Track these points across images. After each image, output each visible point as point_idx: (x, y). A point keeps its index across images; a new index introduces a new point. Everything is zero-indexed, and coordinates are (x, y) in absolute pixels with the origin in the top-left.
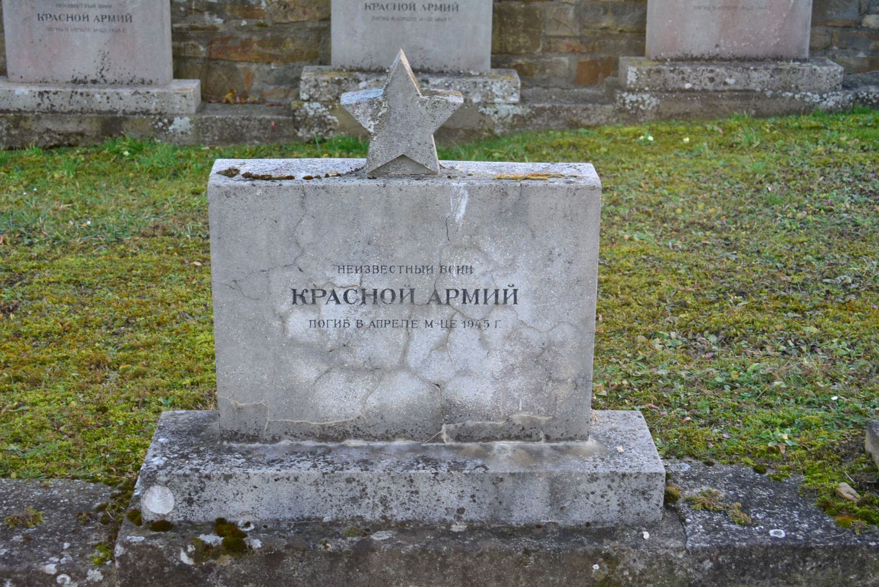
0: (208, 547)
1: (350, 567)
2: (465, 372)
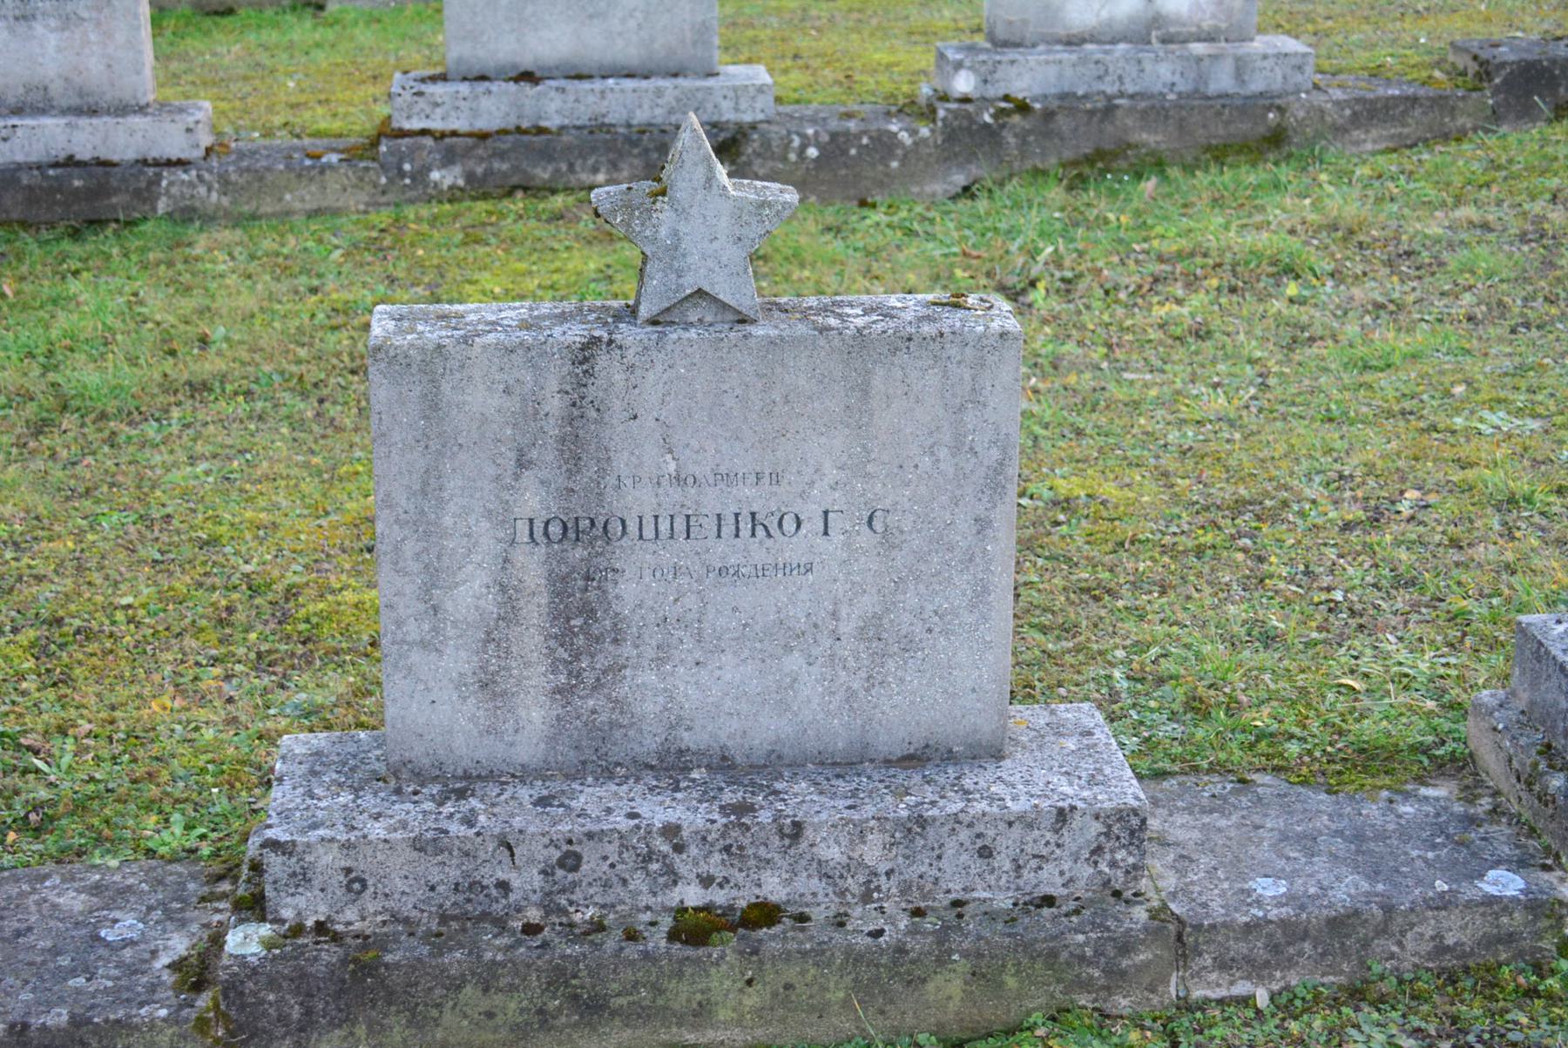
0: (1003, 110)
1: (1102, 121)
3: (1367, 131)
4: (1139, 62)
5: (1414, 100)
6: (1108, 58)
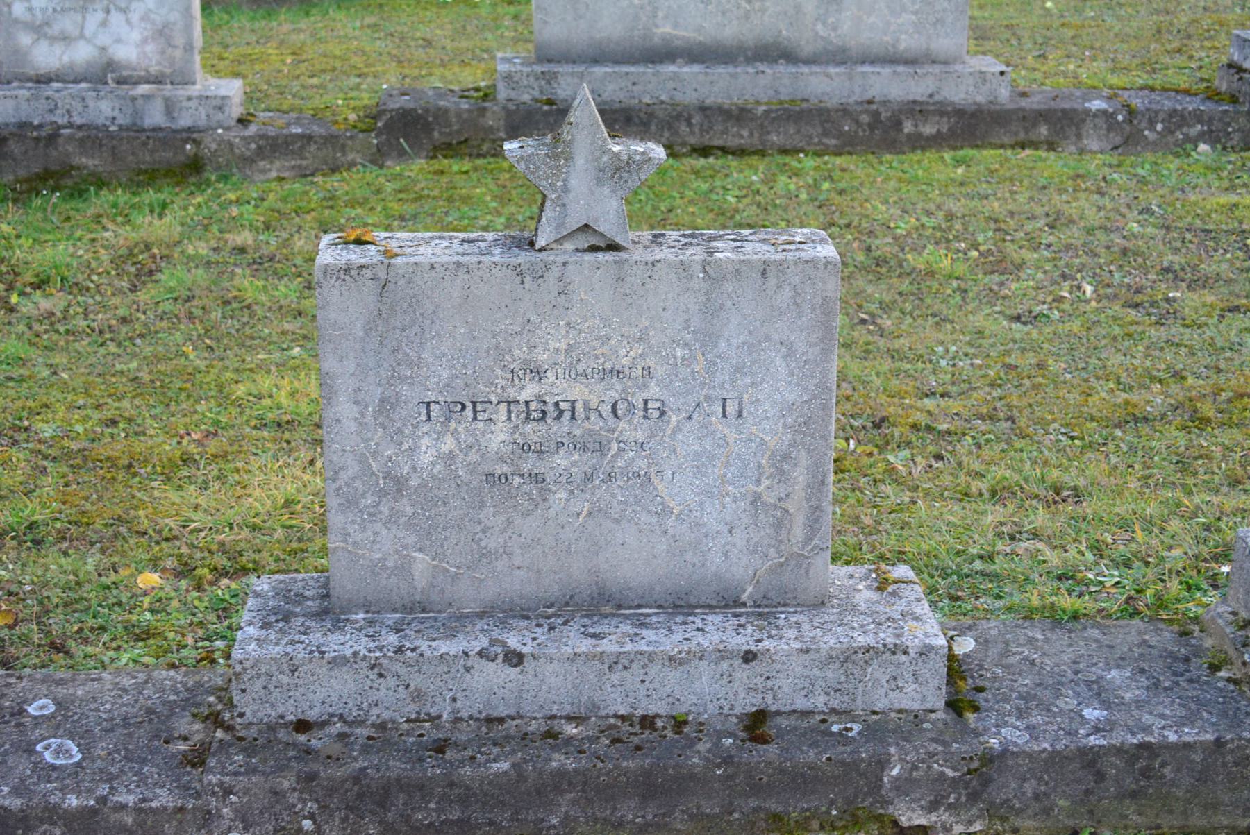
1: (47, 146)
2: (118, 41)
3: (271, 162)
4: (83, 99)
5: (308, 138)
6: (57, 95)
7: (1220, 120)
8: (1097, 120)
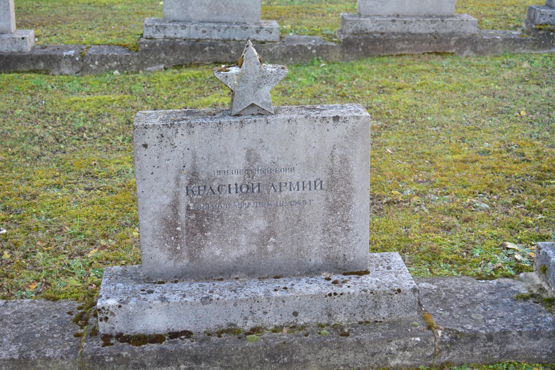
7: (125, 59)
8: (66, 60)
